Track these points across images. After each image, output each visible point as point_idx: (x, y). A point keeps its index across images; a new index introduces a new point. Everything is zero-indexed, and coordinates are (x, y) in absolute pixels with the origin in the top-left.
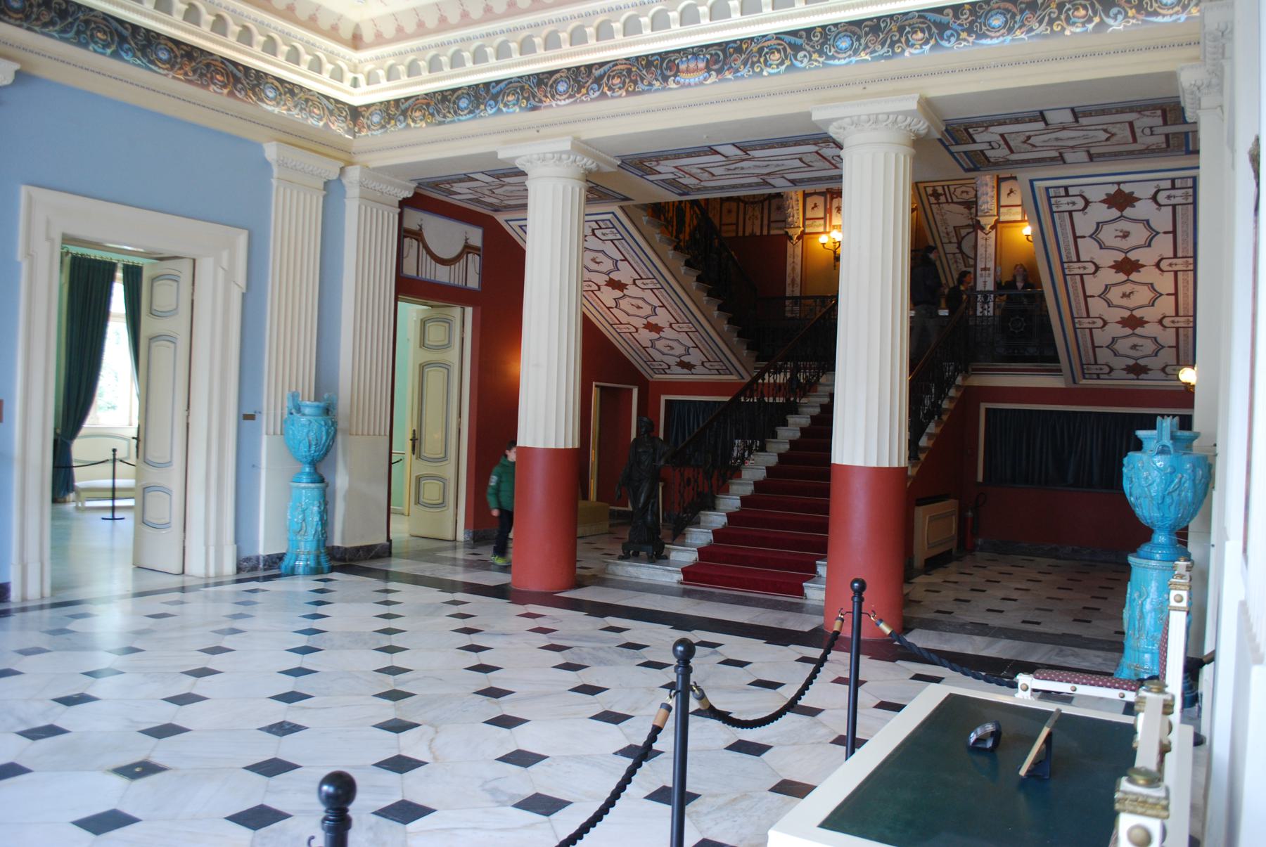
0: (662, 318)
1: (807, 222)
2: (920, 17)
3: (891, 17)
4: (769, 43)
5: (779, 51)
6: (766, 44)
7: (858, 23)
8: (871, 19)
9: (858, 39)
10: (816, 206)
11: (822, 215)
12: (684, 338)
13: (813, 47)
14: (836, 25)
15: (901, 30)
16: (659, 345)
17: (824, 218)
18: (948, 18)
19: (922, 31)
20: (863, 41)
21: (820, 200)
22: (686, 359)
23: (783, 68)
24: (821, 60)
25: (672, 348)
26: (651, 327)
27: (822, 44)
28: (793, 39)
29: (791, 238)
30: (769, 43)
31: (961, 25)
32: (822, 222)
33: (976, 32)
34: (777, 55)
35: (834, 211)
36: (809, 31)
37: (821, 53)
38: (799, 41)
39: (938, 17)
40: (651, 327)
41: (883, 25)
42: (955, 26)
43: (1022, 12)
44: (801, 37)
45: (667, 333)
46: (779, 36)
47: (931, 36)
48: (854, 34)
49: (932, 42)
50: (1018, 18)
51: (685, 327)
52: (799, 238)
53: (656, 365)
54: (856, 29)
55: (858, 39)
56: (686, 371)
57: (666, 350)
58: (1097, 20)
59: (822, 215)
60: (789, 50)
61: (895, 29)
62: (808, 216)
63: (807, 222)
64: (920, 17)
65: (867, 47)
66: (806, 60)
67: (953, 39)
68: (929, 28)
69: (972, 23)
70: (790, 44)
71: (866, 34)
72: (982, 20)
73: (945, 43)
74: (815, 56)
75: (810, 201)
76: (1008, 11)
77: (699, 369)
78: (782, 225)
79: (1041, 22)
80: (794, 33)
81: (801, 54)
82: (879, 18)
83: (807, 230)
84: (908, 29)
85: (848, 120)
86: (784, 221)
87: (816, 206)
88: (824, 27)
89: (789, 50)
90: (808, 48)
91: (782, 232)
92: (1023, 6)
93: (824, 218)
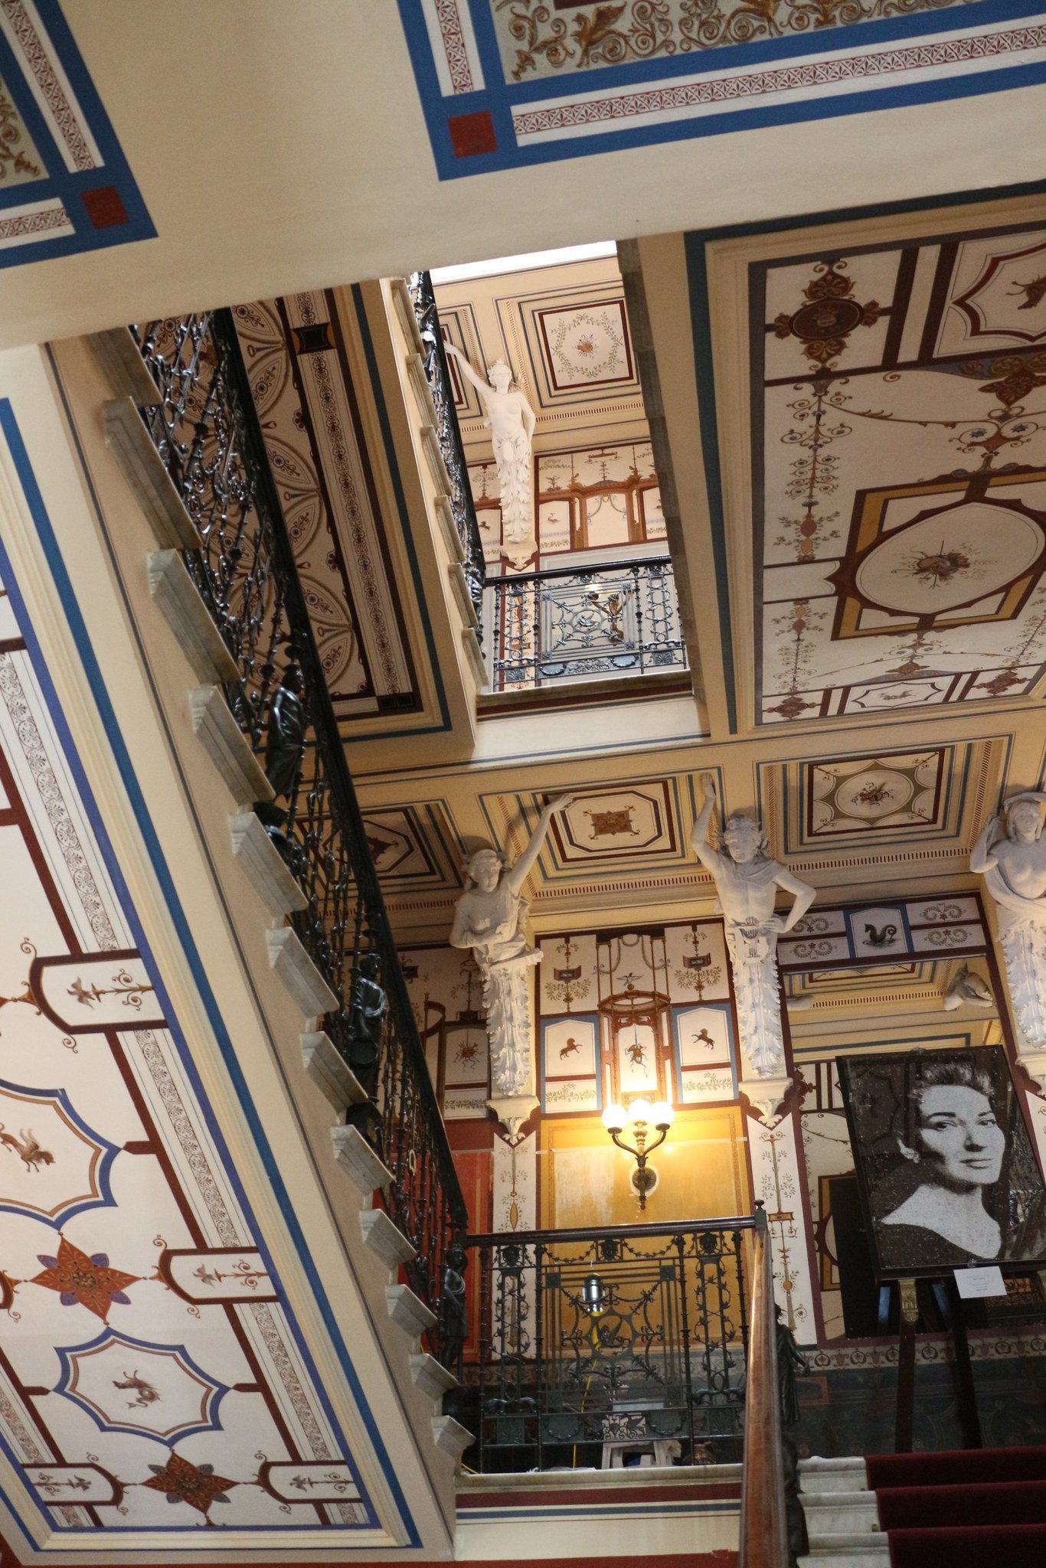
0: (132, 1228)
1: (550, 1088)
10: (571, 1045)
11: (590, 1068)
12: (210, 1338)
16: (97, 1375)
17: (597, 1076)
21: (583, 1033)
22: (194, 1451)
25: (146, 1393)
26: (83, 1278)
29: (503, 1129)
32: (591, 1085)
35: (624, 1058)
40: (83, 1278)
45: (146, 1310)
51: (230, 1276)
52: (526, 1129)
53: (63, 1485)
56: (185, 1512)
57: (118, 1406)
59: (590, 1068)
62: (551, 1070)
63: (550, 1088)
75: (556, 1036)
77: (245, 1502)
78: (482, 1093)
83: (551, 1108)
86: (487, 1085)
87: (571, 1045)
91: (480, 1113)
93: (597, 1076)
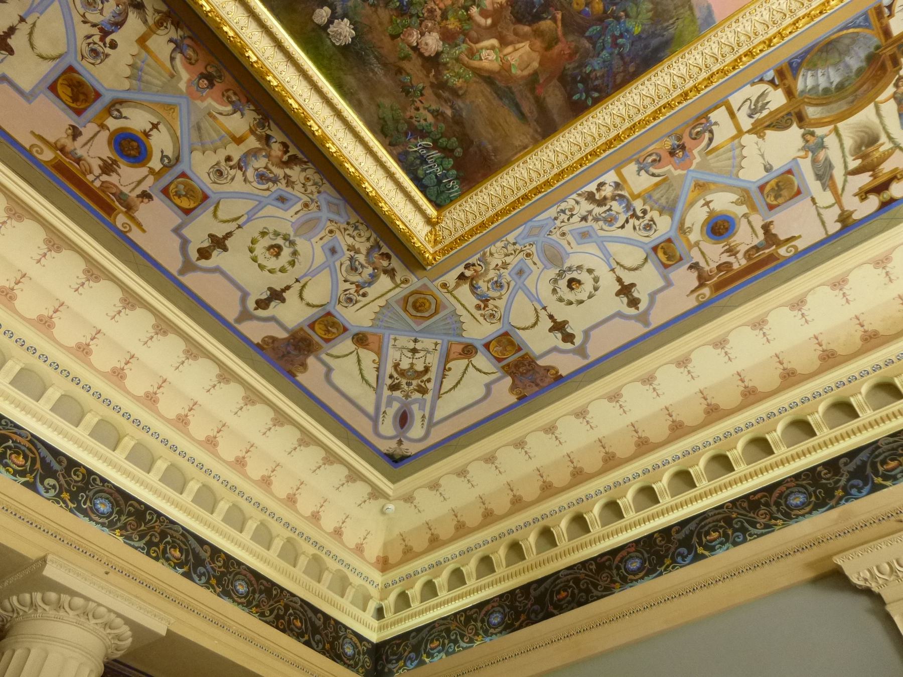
2: (183, 535)
3: (159, 515)
4: (19, 439)
5: (26, 457)
6: (15, 437)
7: (128, 497)
8: (140, 503)
9: (120, 513)
13: (68, 484)
14: (104, 480)
15: (163, 535)
18: (205, 555)
19: (181, 551)
20: (123, 518)
23: (23, 480)
24: (71, 505)
27: (81, 489)
28: (49, 458)
30: (15, 437)
31: (214, 570)
33: (223, 586)
34: (21, 460)
36: (72, 464)
37: (74, 498)
38: (56, 466)
41: (148, 517)
42: (208, 567)
43: (261, 593)
44: (60, 462)
46: (35, 440)
47: (187, 562)
48: (118, 505)
49: (185, 569)
50: (257, 596)
54: (122, 502)
55: (120, 513)
58: (306, 637)
60: (38, 465)
61: (157, 529)
64: (183, 535)
65: (123, 528)
66: (52, 493)
67: (204, 579)
68: (187, 551)
69: (223, 574)
70: (43, 460)
71: (130, 514)
72: (231, 577)
73: (196, 579)
74: (66, 496)
76: (252, 585)
79: (271, 612)
80: (56, 453)
81: (50, 481)
82: (148, 507)
84: (169, 539)
85: (78, 601)
88: (90, 472)
89: (38, 465)
90: (63, 481)
92: (263, 588)
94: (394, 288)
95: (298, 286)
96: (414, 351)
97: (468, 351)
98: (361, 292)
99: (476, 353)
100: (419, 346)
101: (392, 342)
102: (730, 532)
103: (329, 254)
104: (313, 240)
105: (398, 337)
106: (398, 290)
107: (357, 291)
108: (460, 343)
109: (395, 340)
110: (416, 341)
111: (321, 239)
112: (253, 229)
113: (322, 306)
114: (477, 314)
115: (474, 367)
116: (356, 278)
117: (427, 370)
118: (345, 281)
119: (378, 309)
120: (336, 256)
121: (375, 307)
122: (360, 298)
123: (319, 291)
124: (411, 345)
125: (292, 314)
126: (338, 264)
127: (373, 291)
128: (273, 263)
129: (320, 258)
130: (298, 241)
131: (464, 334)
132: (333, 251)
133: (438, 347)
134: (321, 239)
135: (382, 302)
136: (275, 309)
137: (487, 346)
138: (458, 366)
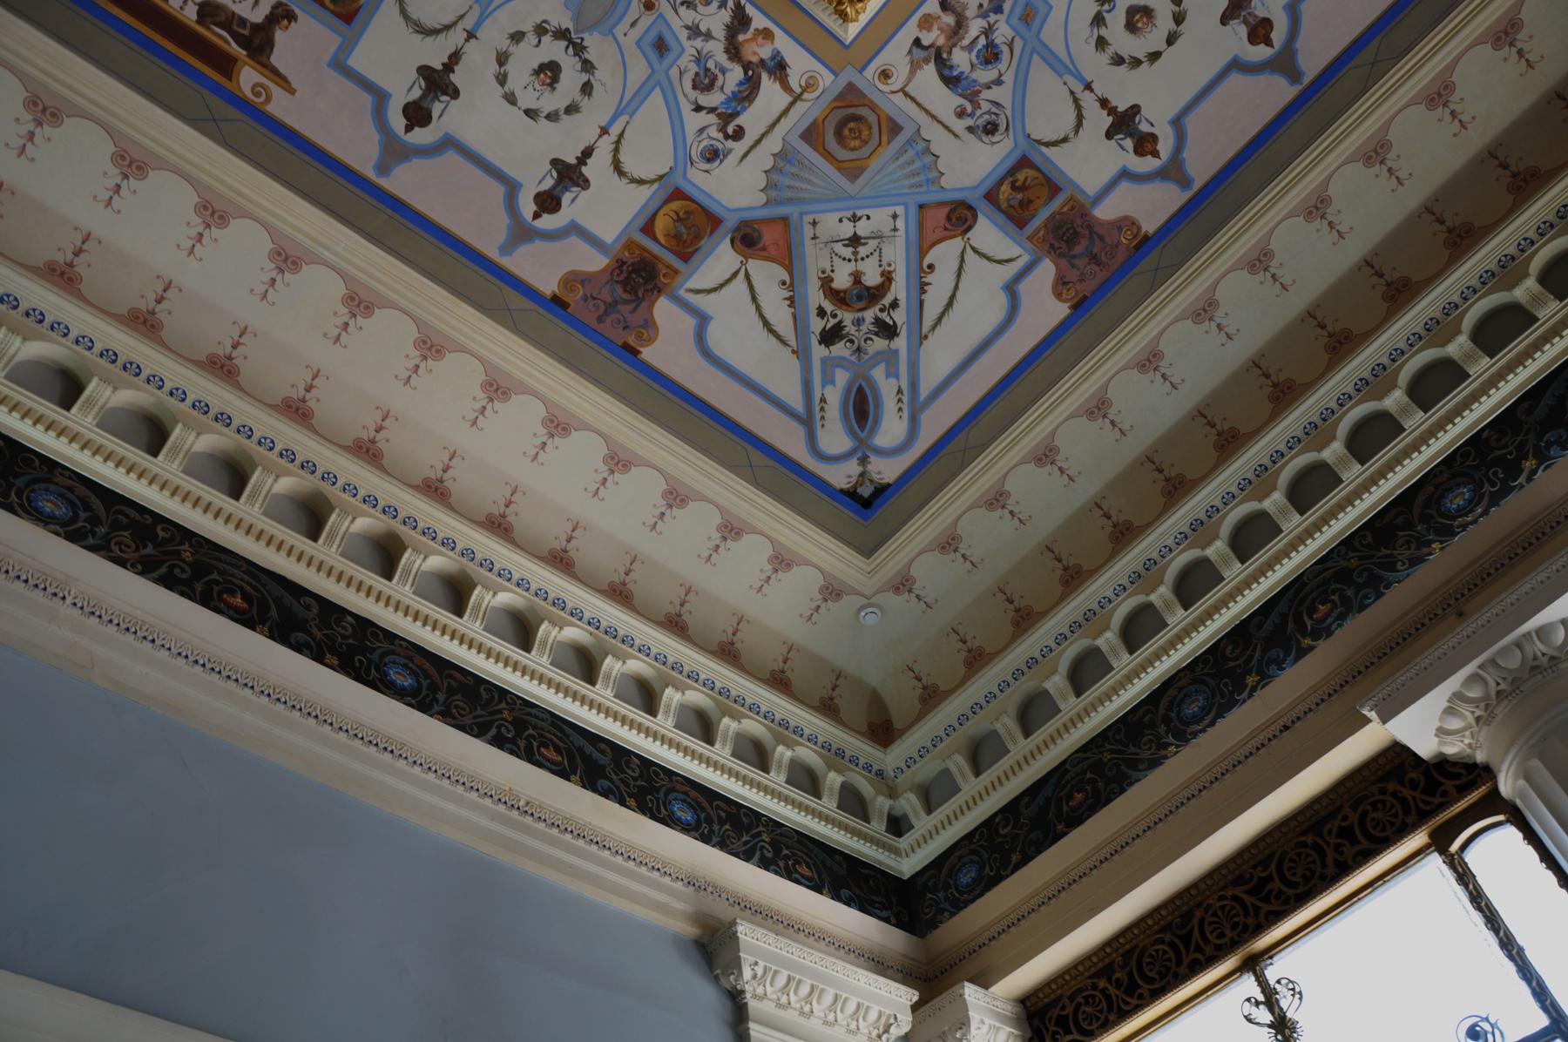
39: (589, 749)
94: (792, 104)
95: (604, 147)
96: (855, 241)
97: (959, 217)
98: (730, 130)
99: (975, 217)
100: (863, 228)
101: (808, 231)
102: (1350, 593)
103: (653, 56)
104: (619, 31)
105: (818, 217)
106: (800, 107)
107: (723, 129)
108: (941, 204)
109: (814, 223)
110: (855, 219)
111: (633, 25)
112: (494, 35)
113: (661, 177)
114: (960, 125)
115: (974, 250)
116: (714, 99)
117: (888, 278)
118: (698, 109)
119: (769, 164)
120: (670, 58)
121: (764, 157)
122: (730, 144)
123: (650, 152)
124: (847, 230)
125: (609, 211)
126: (674, 72)
127: (753, 119)
128: (552, 101)
129: (639, 71)
130: (590, 40)
131: (943, 182)
132: (661, 46)
133: (900, 223)
134: (633, 25)
135: (773, 144)
136: (573, 207)
137: (991, 196)
138: (945, 254)
